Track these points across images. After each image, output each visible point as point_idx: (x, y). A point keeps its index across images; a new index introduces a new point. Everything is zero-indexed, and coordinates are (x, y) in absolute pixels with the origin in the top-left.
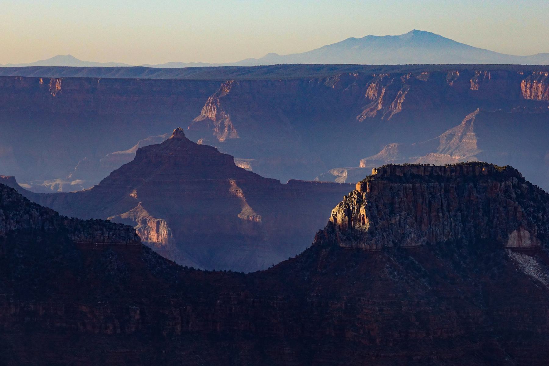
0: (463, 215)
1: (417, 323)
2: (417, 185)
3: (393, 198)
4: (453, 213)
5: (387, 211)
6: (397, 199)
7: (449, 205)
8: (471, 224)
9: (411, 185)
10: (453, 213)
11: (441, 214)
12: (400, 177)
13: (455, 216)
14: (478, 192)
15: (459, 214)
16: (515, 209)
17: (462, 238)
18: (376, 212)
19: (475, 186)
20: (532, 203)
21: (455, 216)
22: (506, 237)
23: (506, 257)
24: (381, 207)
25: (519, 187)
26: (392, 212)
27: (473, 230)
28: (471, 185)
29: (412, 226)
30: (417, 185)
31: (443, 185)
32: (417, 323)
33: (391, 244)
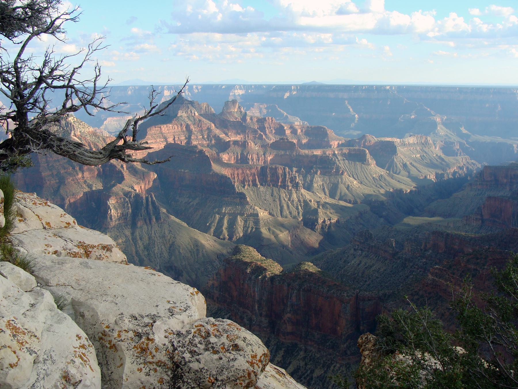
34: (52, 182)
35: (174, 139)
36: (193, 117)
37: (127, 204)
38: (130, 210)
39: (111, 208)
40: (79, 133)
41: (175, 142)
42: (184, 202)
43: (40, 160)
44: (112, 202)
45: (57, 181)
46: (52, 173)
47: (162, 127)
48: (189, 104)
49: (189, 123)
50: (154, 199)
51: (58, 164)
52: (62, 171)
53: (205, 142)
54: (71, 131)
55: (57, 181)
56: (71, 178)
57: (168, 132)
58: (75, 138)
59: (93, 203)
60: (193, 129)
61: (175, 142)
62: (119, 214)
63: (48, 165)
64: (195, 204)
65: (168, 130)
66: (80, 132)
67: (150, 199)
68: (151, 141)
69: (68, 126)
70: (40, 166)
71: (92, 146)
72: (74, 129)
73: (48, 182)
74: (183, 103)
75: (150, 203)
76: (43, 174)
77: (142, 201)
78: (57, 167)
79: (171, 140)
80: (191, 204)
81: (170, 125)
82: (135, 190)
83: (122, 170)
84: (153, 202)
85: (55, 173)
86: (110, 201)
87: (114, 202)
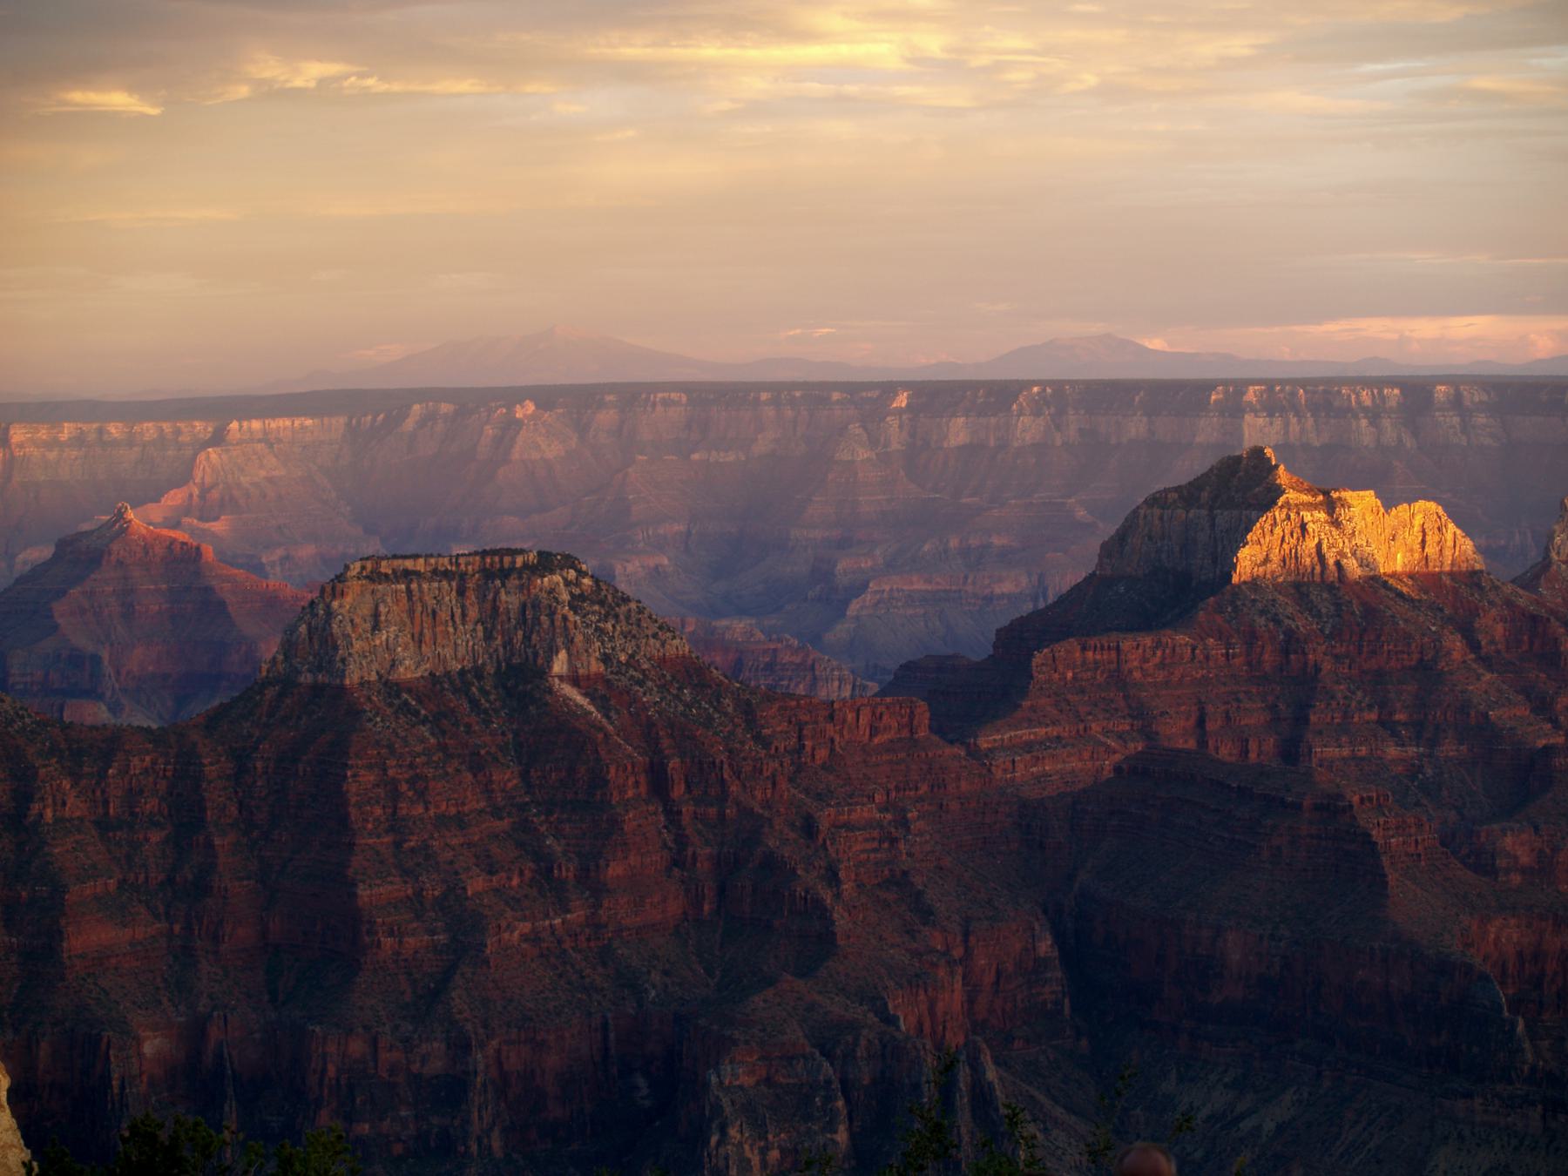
0: (485, 629)
1: (410, 794)
2: (414, 586)
3: (377, 607)
4: (469, 627)
5: (368, 626)
6: (382, 609)
7: (464, 615)
8: (499, 641)
9: (403, 586)
10: (469, 627)
11: (451, 630)
12: (386, 575)
13: (474, 630)
14: (507, 593)
15: (480, 627)
16: (565, 618)
17: (484, 664)
18: (349, 629)
19: (503, 585)
20: (596, 608)
21: (474, 630)
22: (549, 662)
23: (550, 691)
24: (357, 620)
25: (578, 584)
26: (376, 627)
27: (501, 650)
28: (498, 582)
29: (406, 648)
30: (414, 586)
31: (454, 584)
32: (410, 794)
33: (374, 677)
34: (410, 941)
35: (1201, 723)
36: (1330, 587)
37: (829, 1099)
38: (842, 1136)
39: (728, 1110)
40: (596, 667)
41: (1202, 743)
42: (1204, 1113)
43: (353, 811)
44: (736, 1075)
45: (442, 938)
46: (419, 893)
47: (1126, 645)
48: (1312, 507)
49: (1302, 624)
50: (991, 1074)
51: (455, 841)
52: (476, 884)
53: (1392, 751)
54: (552, 651)
55: (442, 938)
56: (526, 927)
57: (1161, 676)
58: (569, 690)
59: (641, 1082)
60: (1327, 666)
61: (1202, 743)
62: (774, 1154)
63: (398, 845)
64: (1269, 1126)
65: (1162, 665)
66: (606, 659)
67: (963, 1075)
68: (1053, 731)
69: (537, 621)
70: (351, 845)
71: (666, 743)
72: (570, 642)
73: (388, 942)
74: (1274, 502)
75: (963, 1100)
76: (363, 892)
77: (916, 1087)
78: (449, 855)
79: (1176, 732)
80: (1247, 1125)
81: (1182, 639)
82: (890, 1020)
83: (827, 896)
84: (982, 1097)
85: (433, 890)
86: (727, 1068)
87: (748, 1081)
